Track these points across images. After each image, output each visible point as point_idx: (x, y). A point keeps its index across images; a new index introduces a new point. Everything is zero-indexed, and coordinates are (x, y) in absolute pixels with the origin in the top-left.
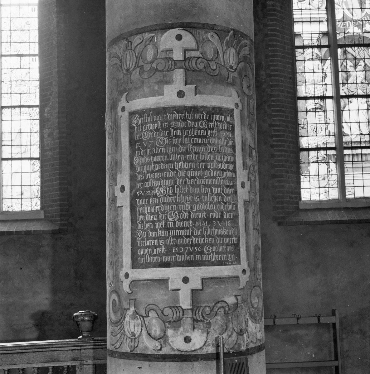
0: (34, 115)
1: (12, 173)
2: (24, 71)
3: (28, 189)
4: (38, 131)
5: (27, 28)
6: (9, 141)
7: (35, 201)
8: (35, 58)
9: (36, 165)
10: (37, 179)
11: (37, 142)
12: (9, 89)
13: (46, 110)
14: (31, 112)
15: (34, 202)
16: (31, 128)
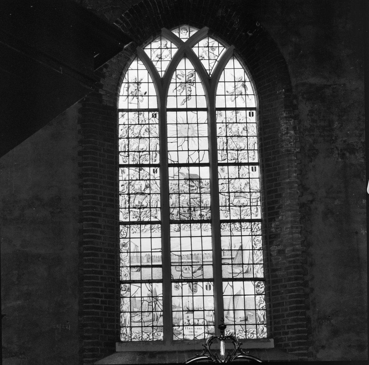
0: (256, 230)
1: (234, 295)
2: (243, 182)
3: (252, 314)
4: (261, 248)
5: (245, 134)
6: (229, 259)
7: (261, 327)
8: (255, 167)
9: (261, 287)
10: (262, 302)
11: (261, 261)
12: (227, 201)
13: (273, 225)
14: (253, 226)
15: (260, 329)
16: (253, 245)
